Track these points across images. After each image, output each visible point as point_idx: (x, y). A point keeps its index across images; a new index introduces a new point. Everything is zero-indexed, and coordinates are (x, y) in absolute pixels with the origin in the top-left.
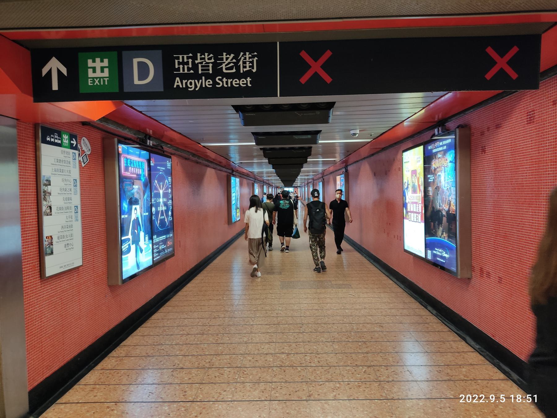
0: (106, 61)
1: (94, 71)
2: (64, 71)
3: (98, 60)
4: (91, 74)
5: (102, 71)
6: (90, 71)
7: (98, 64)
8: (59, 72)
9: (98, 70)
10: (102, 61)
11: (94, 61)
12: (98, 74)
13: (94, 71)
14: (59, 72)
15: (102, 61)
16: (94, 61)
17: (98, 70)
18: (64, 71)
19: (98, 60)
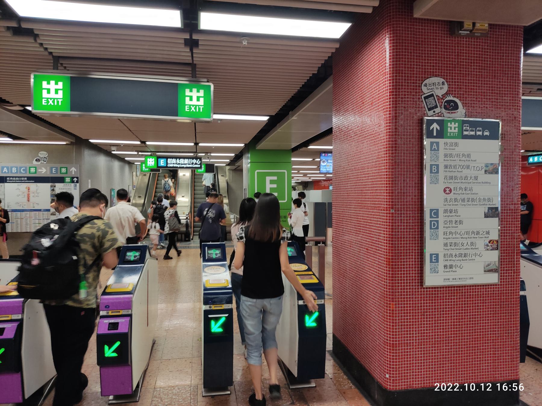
0: (457, 124)
1: (451, 129)
2: (439, 128)
3: (453, 123)
4: (449, 130)
5: (455, 129)
6: (449, 128)
7: (453, 125)
8: (437, 129)
9: (453, 128)
10: (455, 124)
11: (451, 124)
12: (453, 130)
13: (451, 129)
14: (437, 129)
15: (455, 124)
16: (451, 124)
17: (453, 128)
18: (439, 128)
19: (453, 123)
